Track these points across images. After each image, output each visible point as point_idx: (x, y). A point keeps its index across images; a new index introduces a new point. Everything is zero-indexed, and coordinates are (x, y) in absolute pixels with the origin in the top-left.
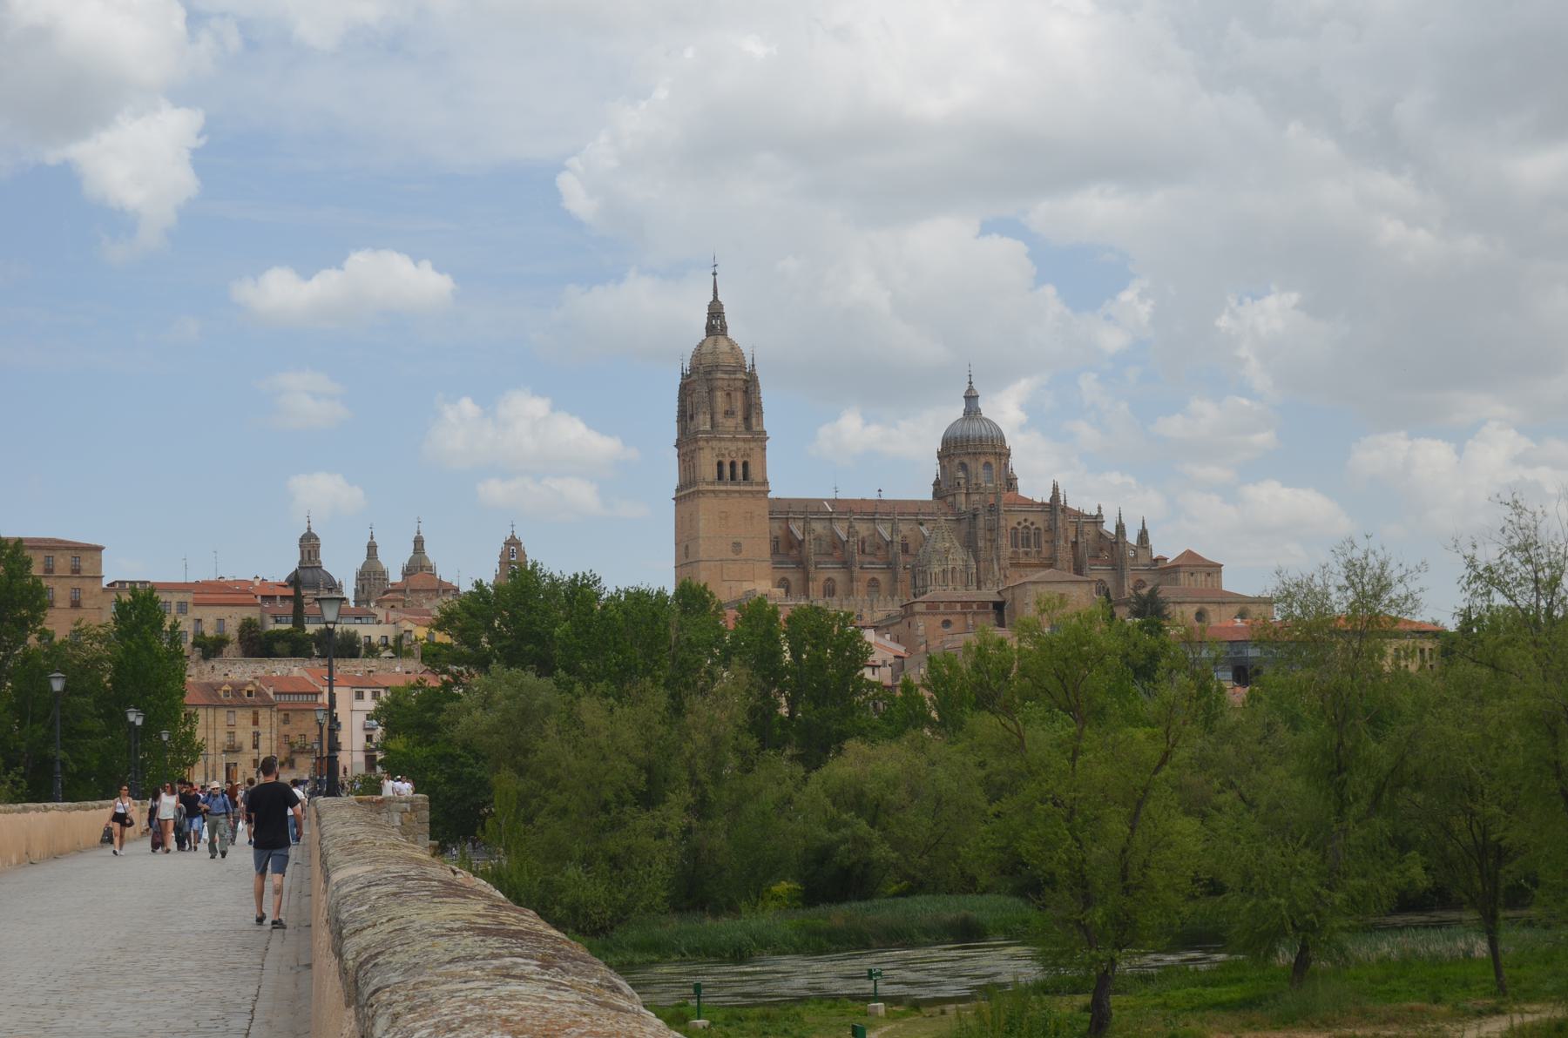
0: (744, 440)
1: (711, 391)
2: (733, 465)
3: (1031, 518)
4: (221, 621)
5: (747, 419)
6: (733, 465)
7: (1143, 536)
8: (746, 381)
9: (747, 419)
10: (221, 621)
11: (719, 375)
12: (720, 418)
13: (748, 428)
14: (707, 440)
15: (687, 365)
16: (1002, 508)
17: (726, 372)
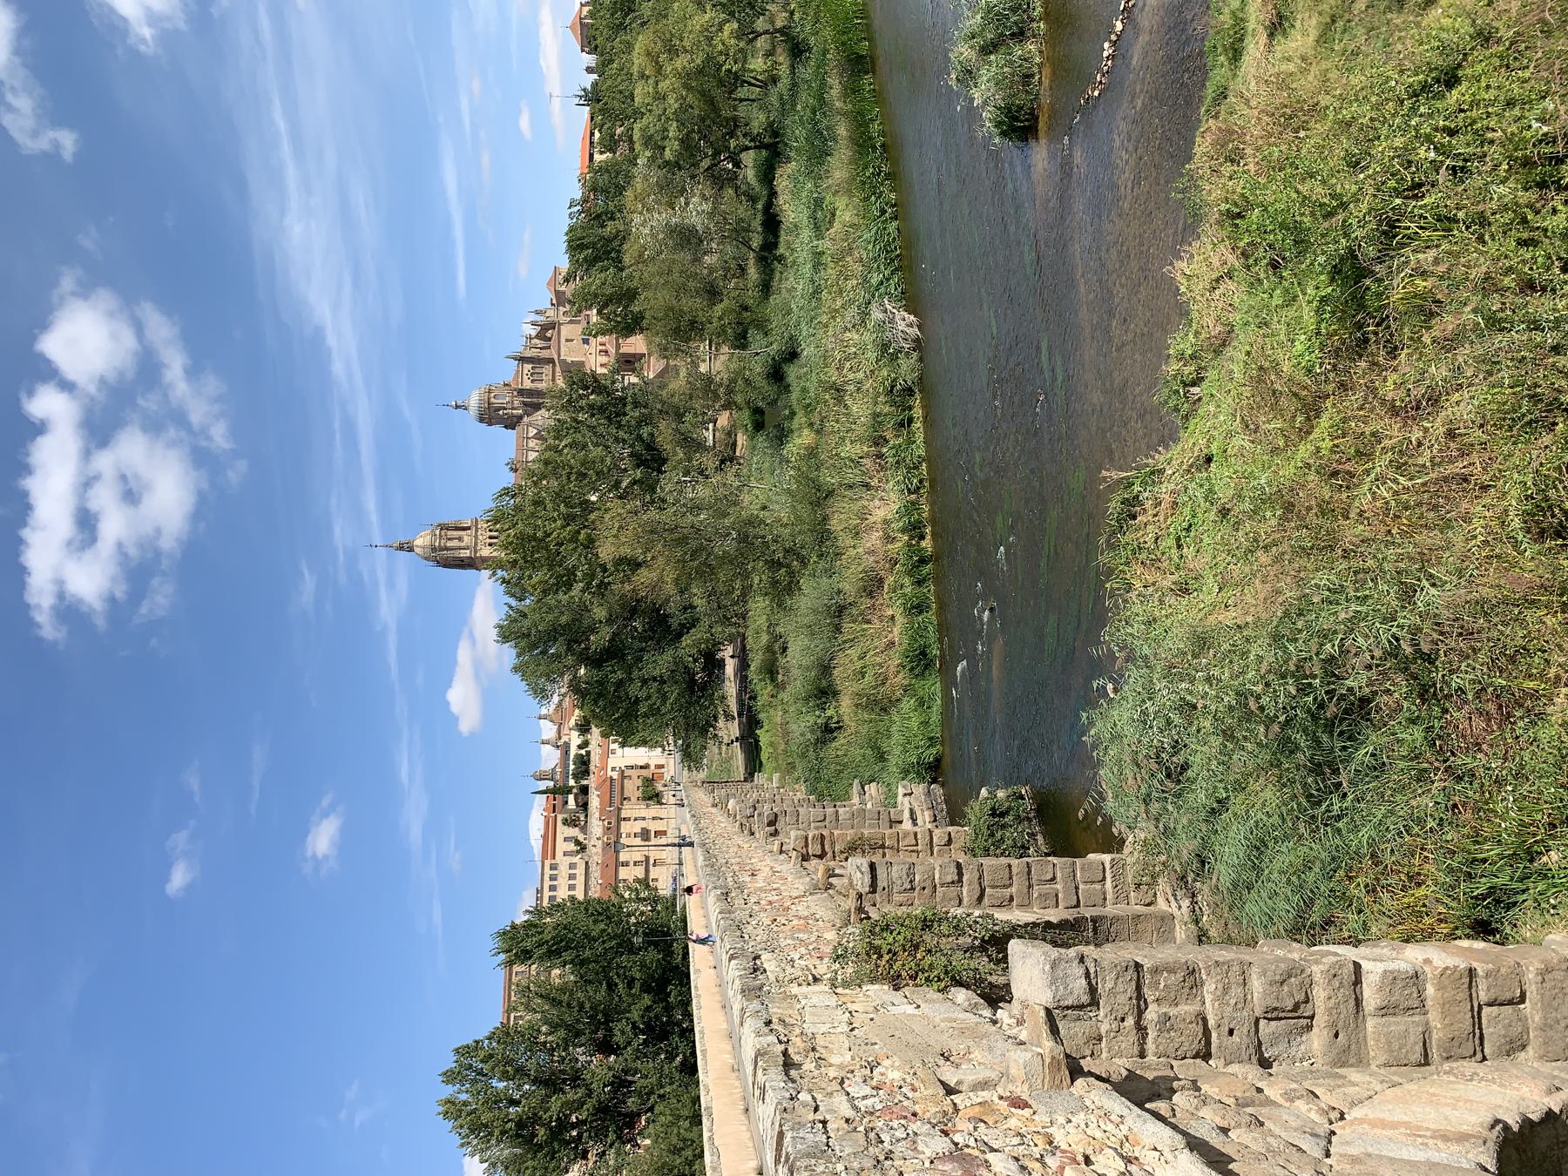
0: (477, 531)
1: (447, 549)
2: (491, 537)
3: (526, 372)
4: (566, 839)
5: (464, 529)
6: (491, 537)
7: (538, 313)
8: (442, 529)
9: (464, 529)
10: (566, 839)
11: (437, 544)
12: (463, 544)
13: (469, 528)
14: (476, 552)
15: (431, 563)
16: (520, 387)
17: (435, 541)
